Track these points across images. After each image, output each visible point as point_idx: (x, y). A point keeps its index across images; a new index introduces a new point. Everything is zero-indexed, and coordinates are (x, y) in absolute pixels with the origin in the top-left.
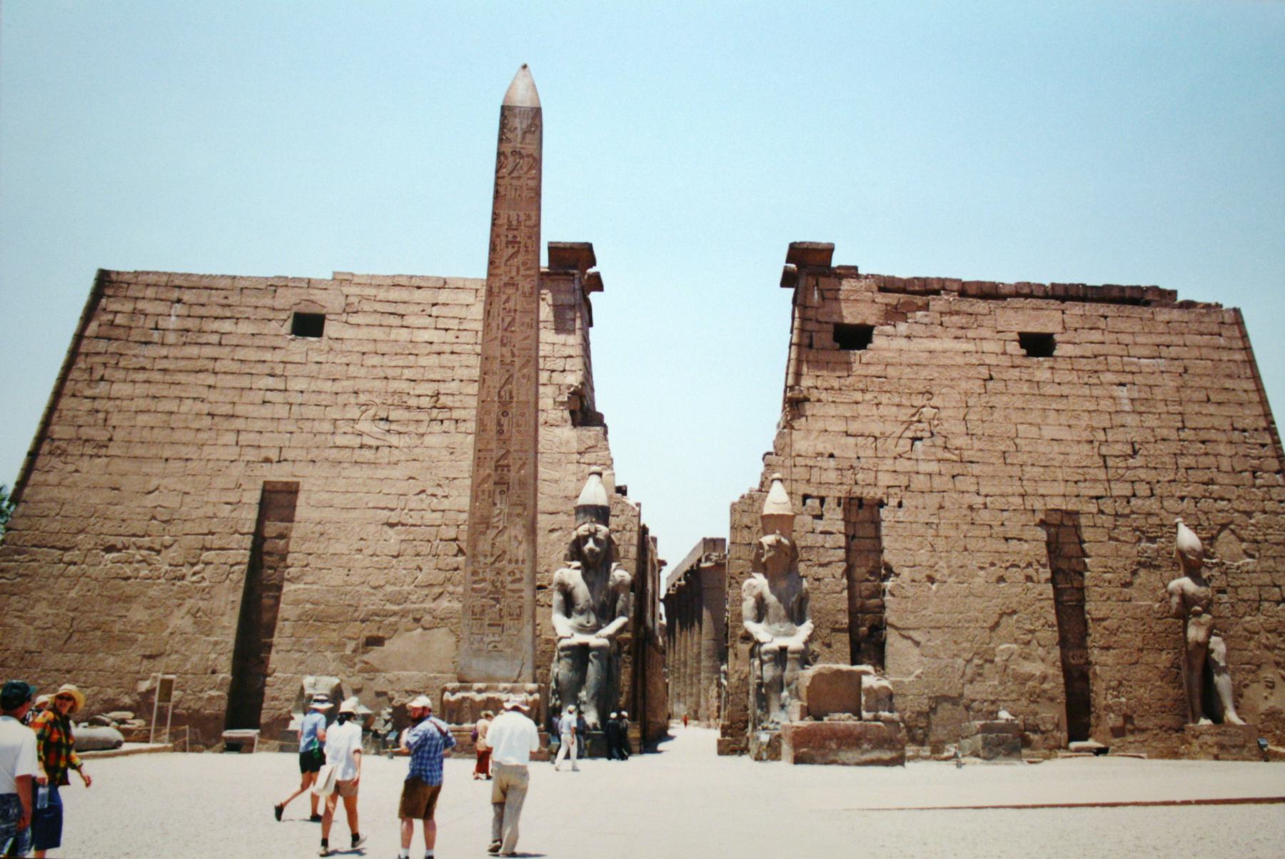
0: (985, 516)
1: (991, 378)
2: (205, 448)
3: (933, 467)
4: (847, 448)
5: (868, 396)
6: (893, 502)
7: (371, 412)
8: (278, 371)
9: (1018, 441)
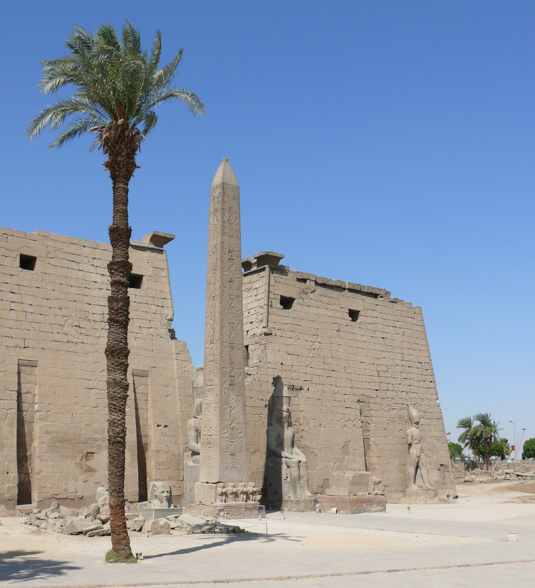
0: (338, 397)
1: (339, 331)
3: (320, 372)
4: (288, 360)
5: (295, 334)
6: (306, 388)
9: (350, 362)
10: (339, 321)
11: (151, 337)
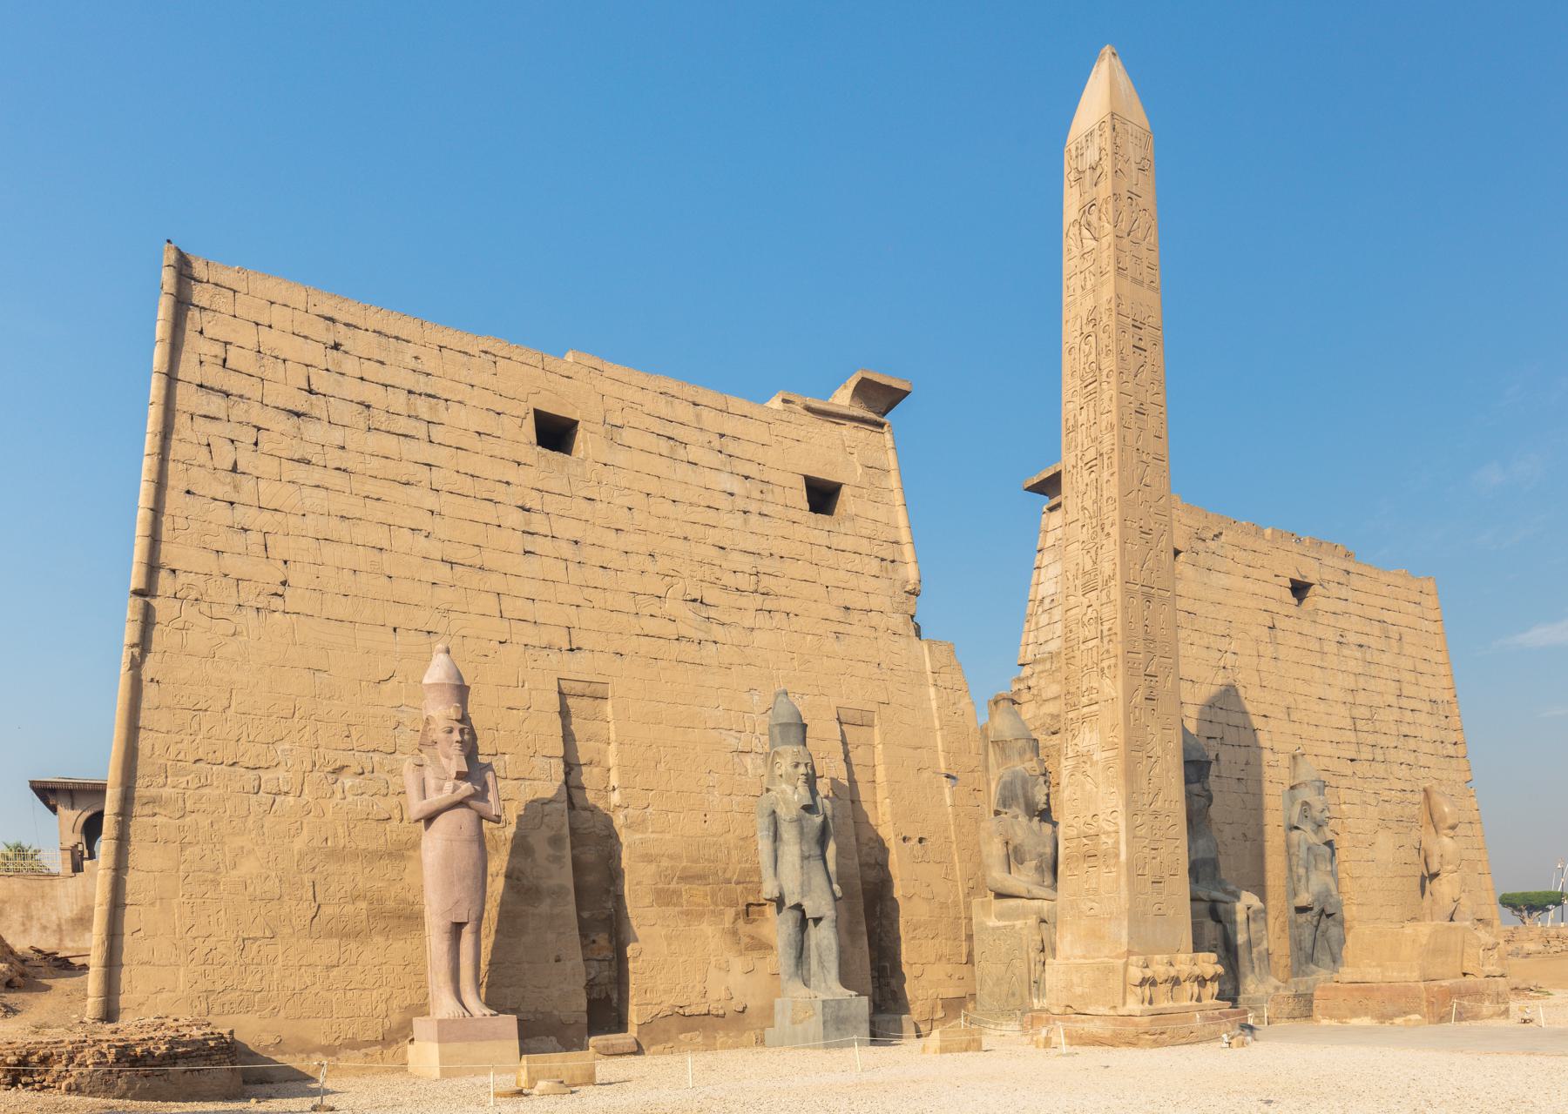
2: (452, 615)
7: (679, 586)
8: (533, 501)
10: (1272, 606)
11: (873, 634)
